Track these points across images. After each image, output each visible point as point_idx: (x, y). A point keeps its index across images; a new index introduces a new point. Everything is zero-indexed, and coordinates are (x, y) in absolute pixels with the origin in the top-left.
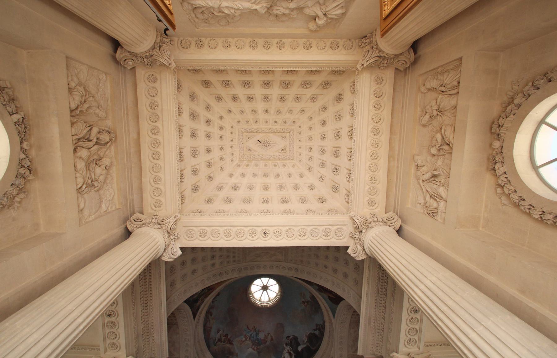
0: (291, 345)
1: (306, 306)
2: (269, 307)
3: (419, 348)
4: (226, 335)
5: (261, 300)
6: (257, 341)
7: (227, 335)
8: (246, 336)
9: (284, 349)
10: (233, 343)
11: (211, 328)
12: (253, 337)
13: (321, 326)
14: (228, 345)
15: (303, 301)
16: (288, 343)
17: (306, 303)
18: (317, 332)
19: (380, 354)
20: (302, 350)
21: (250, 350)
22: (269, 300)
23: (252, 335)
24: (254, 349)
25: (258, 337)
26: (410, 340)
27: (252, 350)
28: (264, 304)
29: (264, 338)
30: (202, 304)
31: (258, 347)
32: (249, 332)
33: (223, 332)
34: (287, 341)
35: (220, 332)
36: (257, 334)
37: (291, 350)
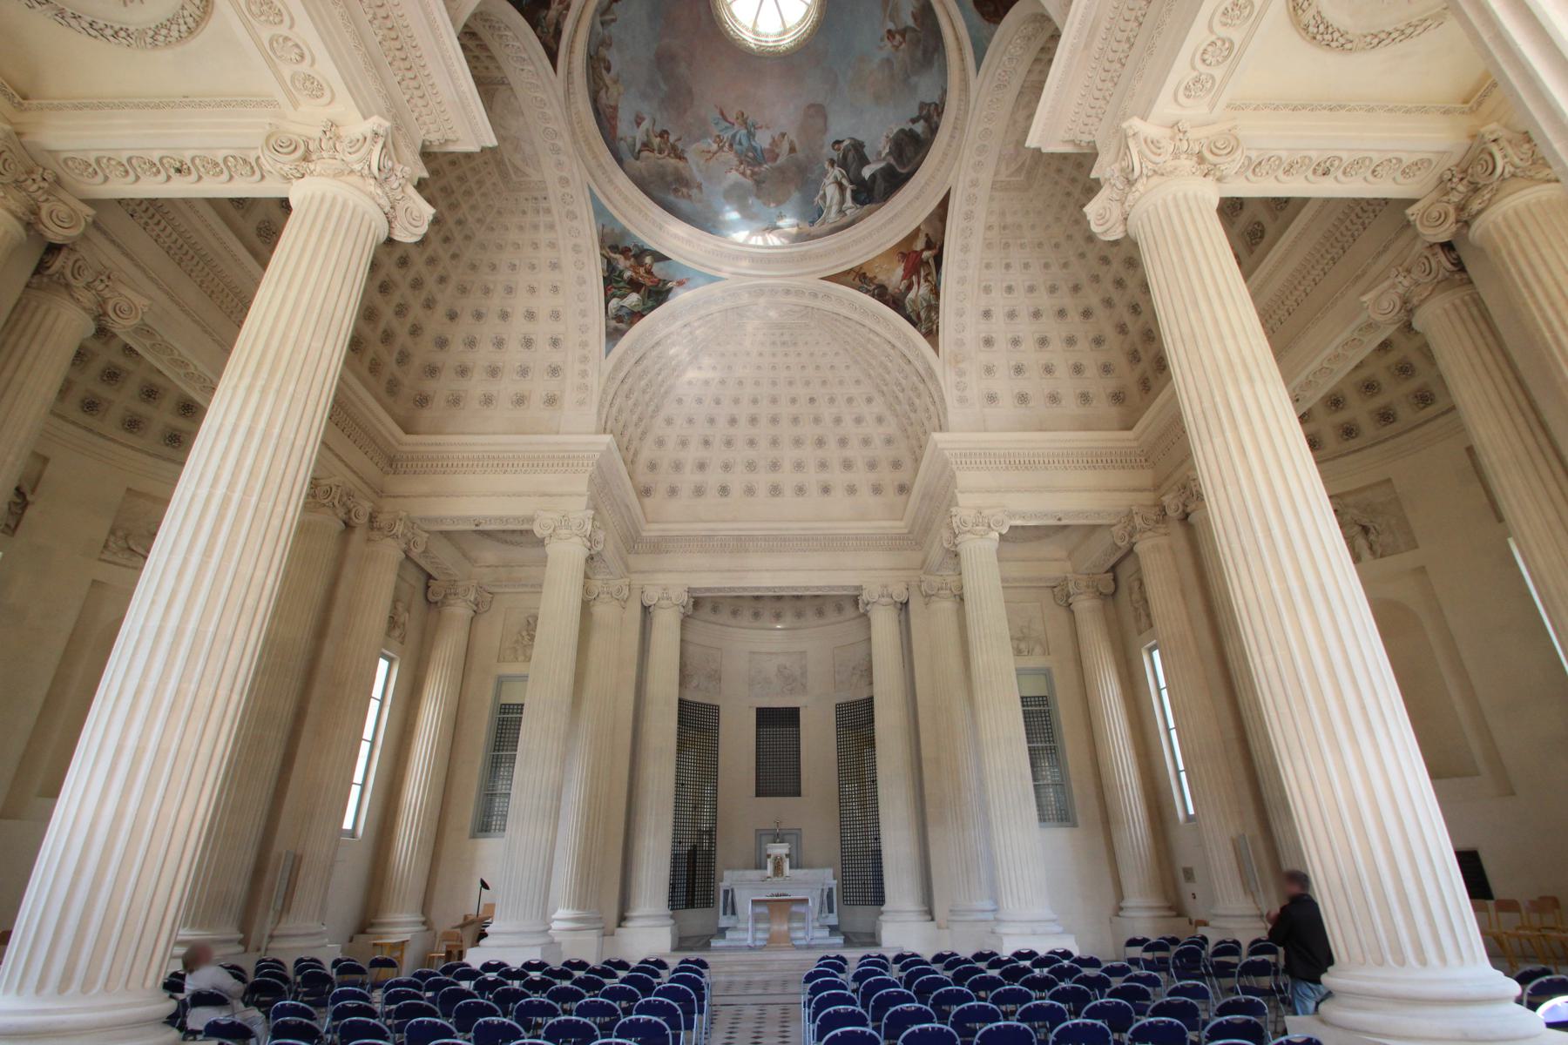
0: (843, 164)
1: (897, 48)
2: (784, 52)
3: (1212, 107)
4: (663, 134)
5: (757, 29)
6: (750, 154)
7: (666, 132)
8: (719, 139)
9: (825, 174)
10: (686, 155)
11: (615, 108)
12: (740, 143)
13: (932, 107)
14: (673, 161)
15: (889, 32)
16: (836, 158)
17: (898, 37)
18: (919, 128)
19: (1090, 138)
20: (873, 176)
21: (734, 176)
22: (782, 29)
23: (737, 138)
24: (743, 174)
25: (753, 143)
26: (1197, 80)
27: (739, 176)
28: (767, 42)
29: (771, 145)
30: (566, 15)
31: (756, 169)
32: (727, 128)
33: (654, 125)
34: (835, 155)
35: (645, 125)
36: (751, 135)
37: (843, 176)
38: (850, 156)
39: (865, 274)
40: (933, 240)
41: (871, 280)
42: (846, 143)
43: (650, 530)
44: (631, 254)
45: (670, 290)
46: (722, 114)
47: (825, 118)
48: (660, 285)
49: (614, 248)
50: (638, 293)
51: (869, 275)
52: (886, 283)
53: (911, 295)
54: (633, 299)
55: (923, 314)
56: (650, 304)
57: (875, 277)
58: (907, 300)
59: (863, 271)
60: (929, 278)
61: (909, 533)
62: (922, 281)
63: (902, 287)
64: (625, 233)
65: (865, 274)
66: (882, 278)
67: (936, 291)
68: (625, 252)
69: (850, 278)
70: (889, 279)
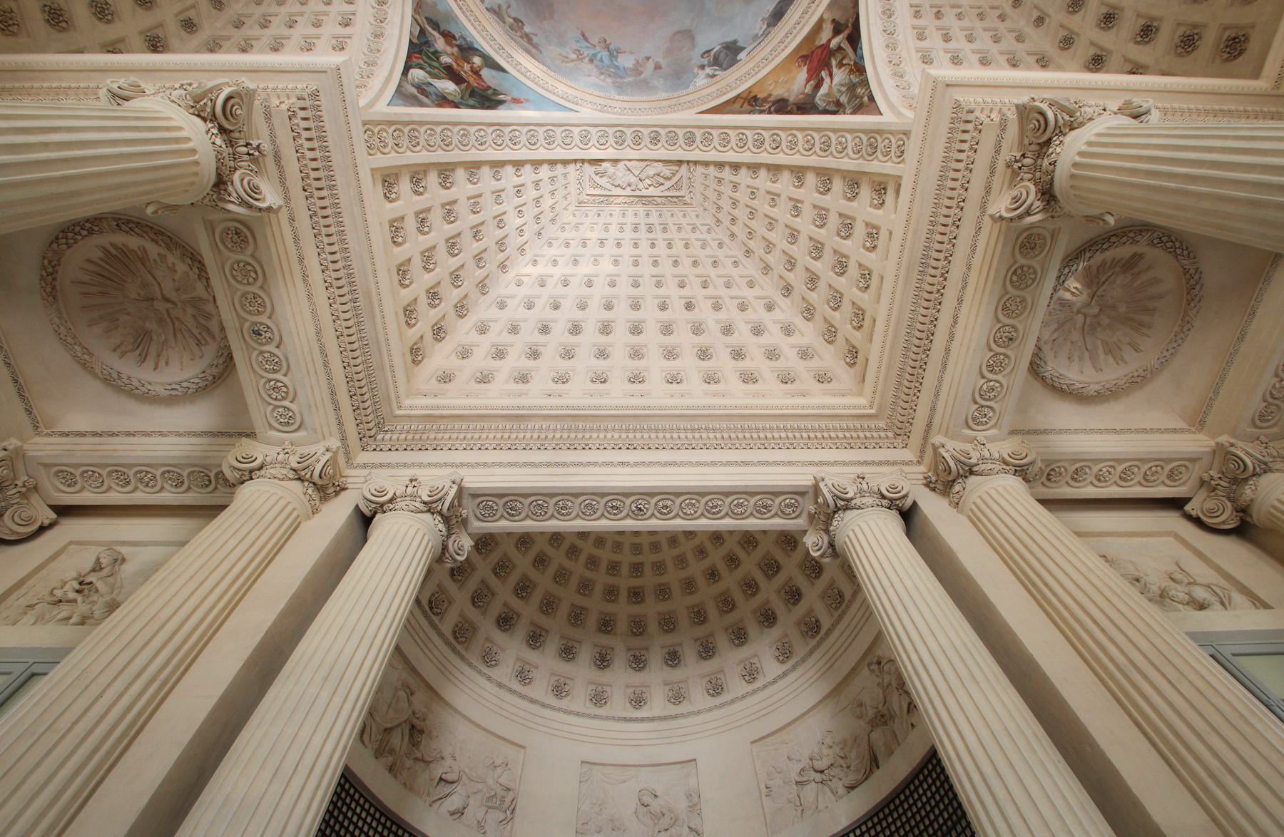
9: (696, 76)
12: (601, 60)
23: (599, 56)
25: (615, 63)
38: (722, 56)
39: (756, 96)
40: (842, 22)
41: (765, 100)
42: (715, 50)
43: (411, 408)
44: (454, 42)
45: (501, 102)
46: (583, 35)
47: (692, 38)
48: (490, 92)
49: (436, 25)
50: (457, 84)
51: (761, 96)
52: (785, 96)
53: (824, 90)
54: (448, 86)
55: (844, 99)
56: (471, 102)
57: (770, 95)
58: (817, 100)
59: (752, 95)
60: (844, 62)
61: (880, 407)
62: (835, 70)
63: (808, 89)
64: (451, 17)
65: (756, 96)
66: (779, 92)
67: (859, 69)
68: (448, 36)
69: (737, 106)
70: (788, 90)
